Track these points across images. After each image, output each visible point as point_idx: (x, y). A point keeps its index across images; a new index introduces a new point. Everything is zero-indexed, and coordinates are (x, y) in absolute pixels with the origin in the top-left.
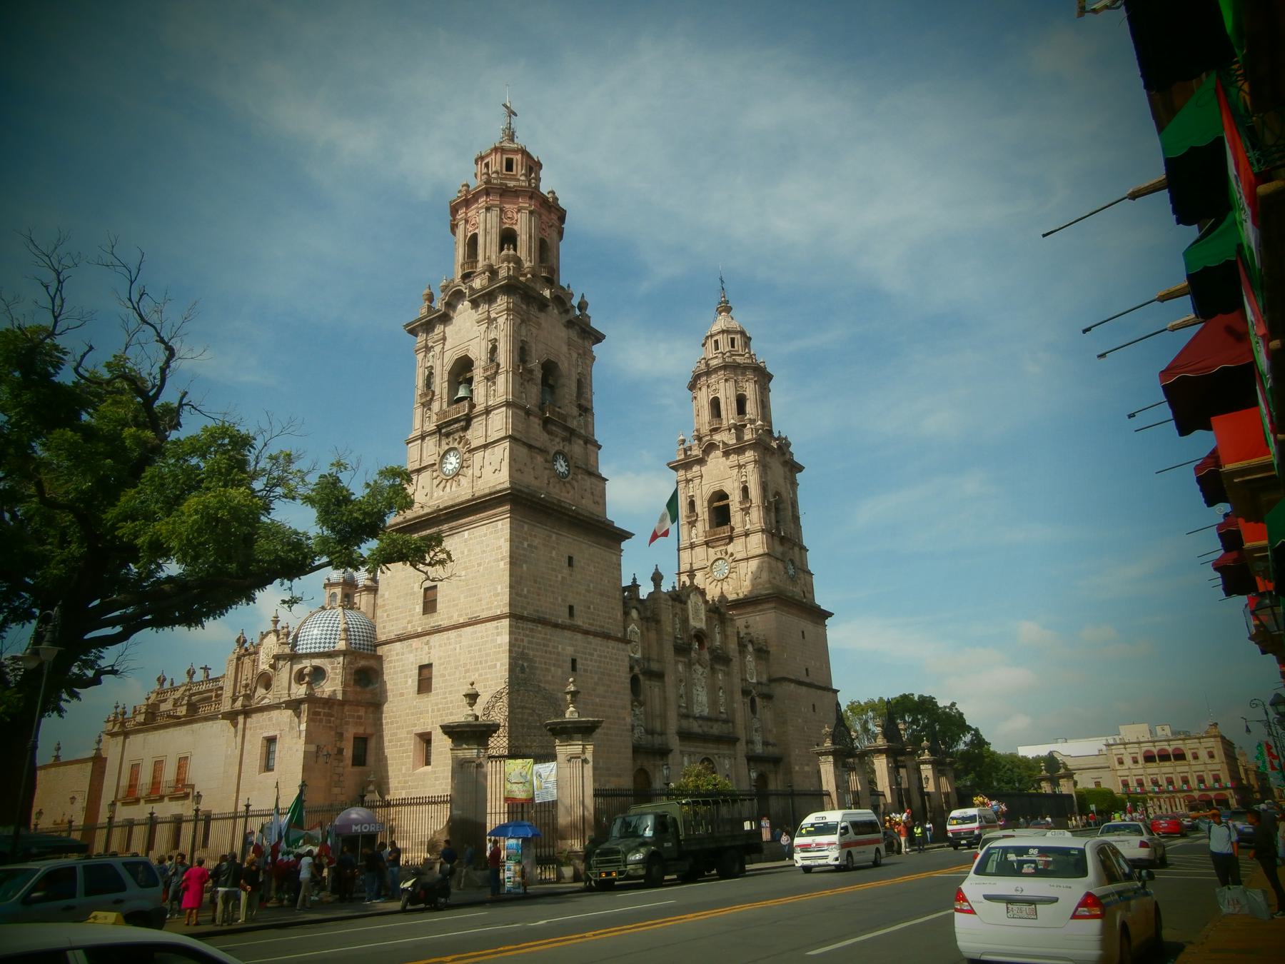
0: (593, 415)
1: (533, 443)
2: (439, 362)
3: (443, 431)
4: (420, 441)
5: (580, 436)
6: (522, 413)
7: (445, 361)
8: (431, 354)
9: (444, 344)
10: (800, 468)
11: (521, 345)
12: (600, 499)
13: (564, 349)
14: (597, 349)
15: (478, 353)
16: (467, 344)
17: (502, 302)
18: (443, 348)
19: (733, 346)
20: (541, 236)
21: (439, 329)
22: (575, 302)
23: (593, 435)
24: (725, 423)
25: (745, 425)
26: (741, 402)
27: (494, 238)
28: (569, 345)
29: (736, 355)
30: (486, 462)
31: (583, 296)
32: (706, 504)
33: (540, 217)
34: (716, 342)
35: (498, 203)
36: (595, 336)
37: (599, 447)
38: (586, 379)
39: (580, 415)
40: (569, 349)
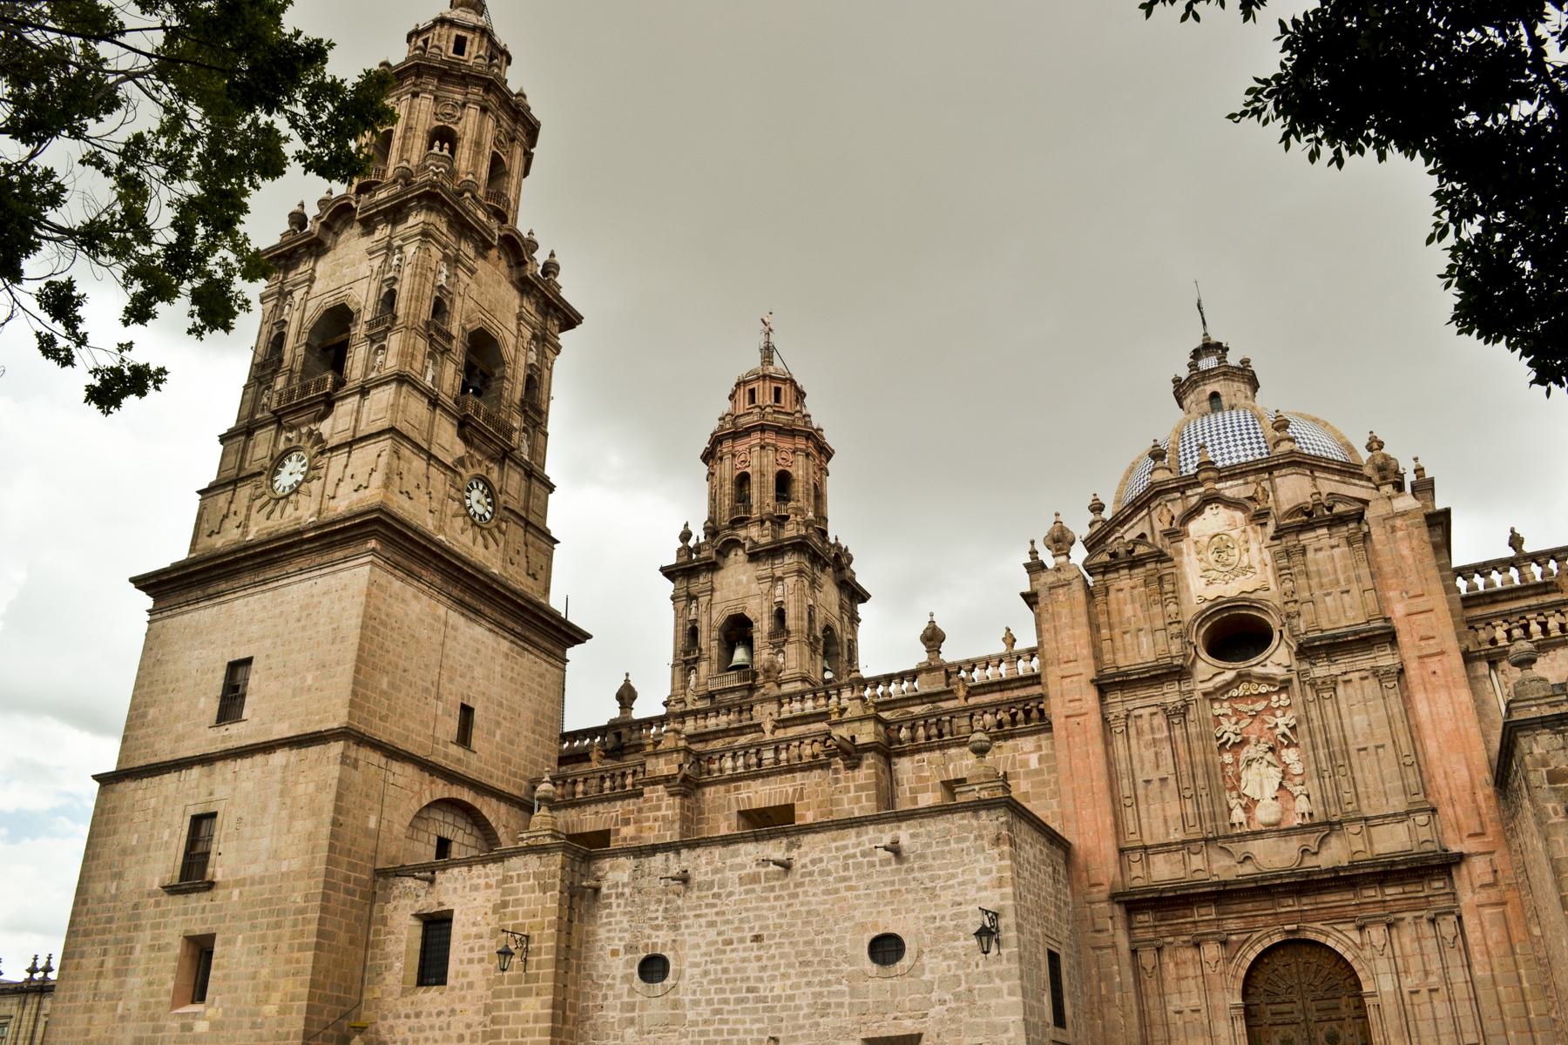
0: (546, 435)
1: (435, 451)
5: (519, 463)
7: (307, 315)
9: (310, 287)
10: (863, 597)
12: (542, 573)
15: (364, 298)
17: (416, 220)
18: (307, 293)
19: (777, 399)
20: (494, 149)
22: (541, 257)
24: (755, 513)
25: (787, 518)
26: (783, 482)
29: (779, 412)
32: (715, 634)
33: (498, 121)
34: (752, 392)
37: (551, 488)
39: (525, 430)
40: (519, 324)
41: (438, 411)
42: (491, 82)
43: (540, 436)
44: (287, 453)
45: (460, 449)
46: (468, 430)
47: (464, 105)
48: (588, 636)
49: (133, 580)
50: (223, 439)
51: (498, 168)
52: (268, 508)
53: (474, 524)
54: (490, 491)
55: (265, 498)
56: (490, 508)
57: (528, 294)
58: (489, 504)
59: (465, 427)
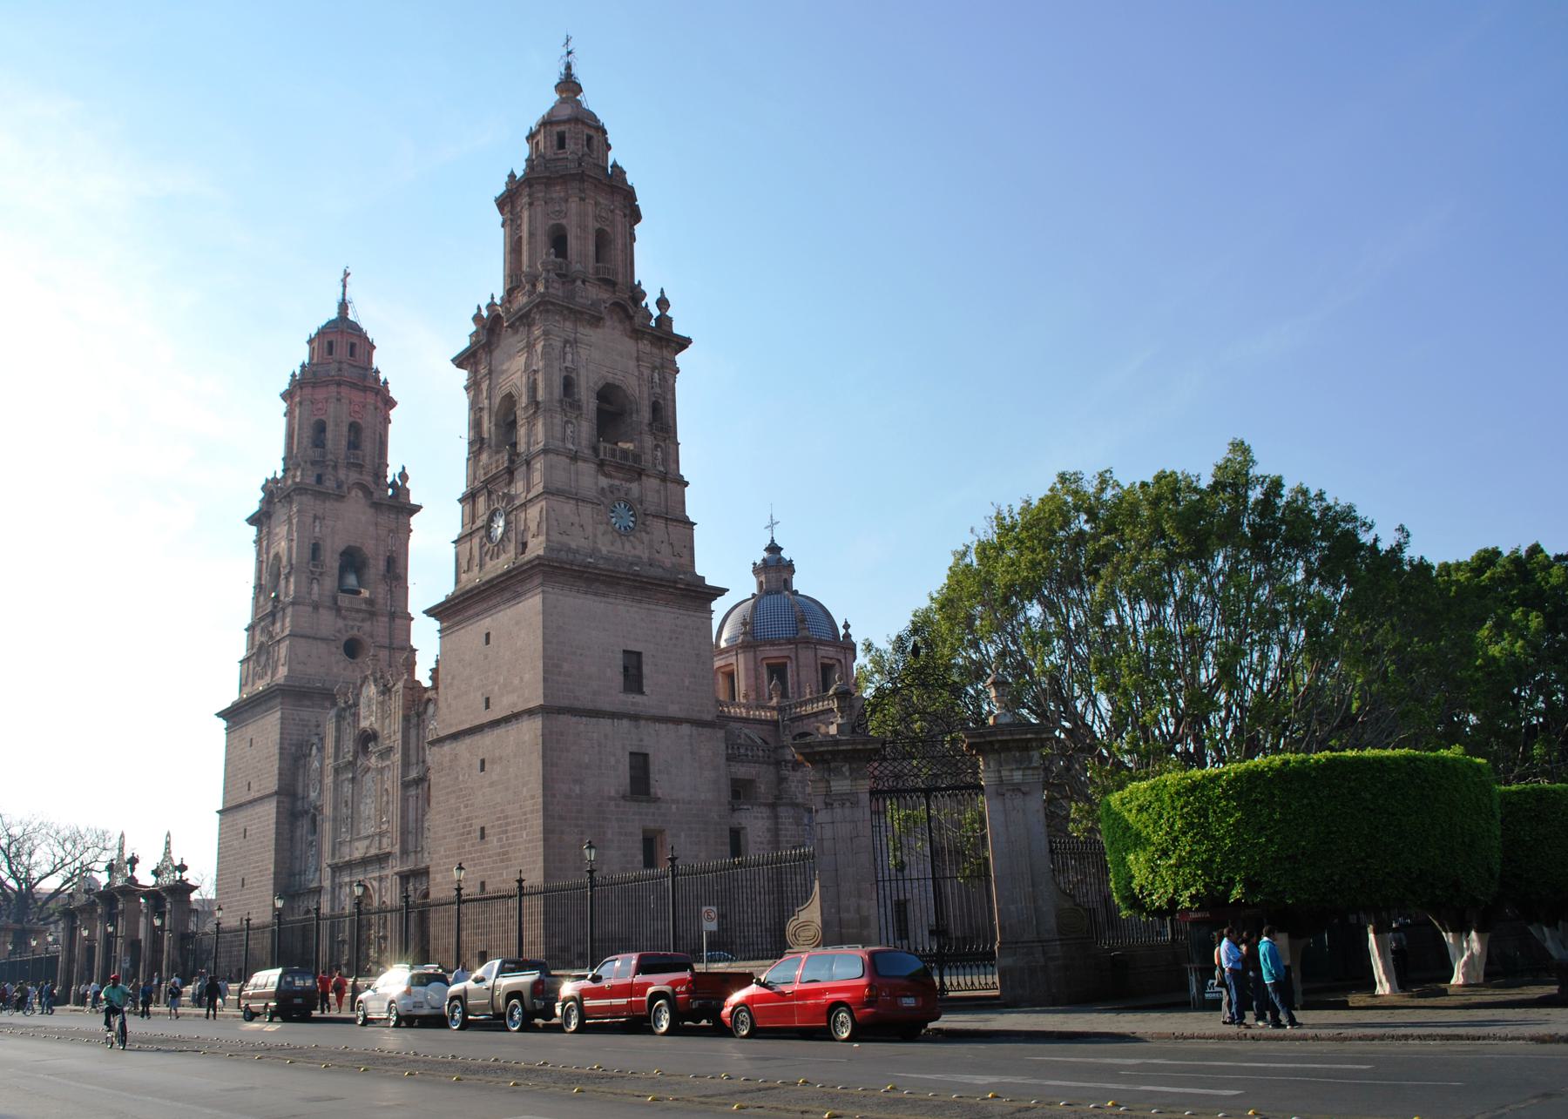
6: (564, 461)
11: (564, 373)
13: (632, 364)
14: (681, 359)
20: (599, 226)
22: (650, 302)
28: (638, 359)
37: (687, 484)
38: (664, 399)
39: (657, 446)
43: (672, 446)
45: (604, 482)
46: (606, 468)
47: (567, 201)
48: (728, 590)
49: (424, 612)
50: (461, 501)
51: (602, 241)
53: (620, 535)
56: (633, 519)
57: (641, 339)
58: (632, 516)
59: (601, 465)
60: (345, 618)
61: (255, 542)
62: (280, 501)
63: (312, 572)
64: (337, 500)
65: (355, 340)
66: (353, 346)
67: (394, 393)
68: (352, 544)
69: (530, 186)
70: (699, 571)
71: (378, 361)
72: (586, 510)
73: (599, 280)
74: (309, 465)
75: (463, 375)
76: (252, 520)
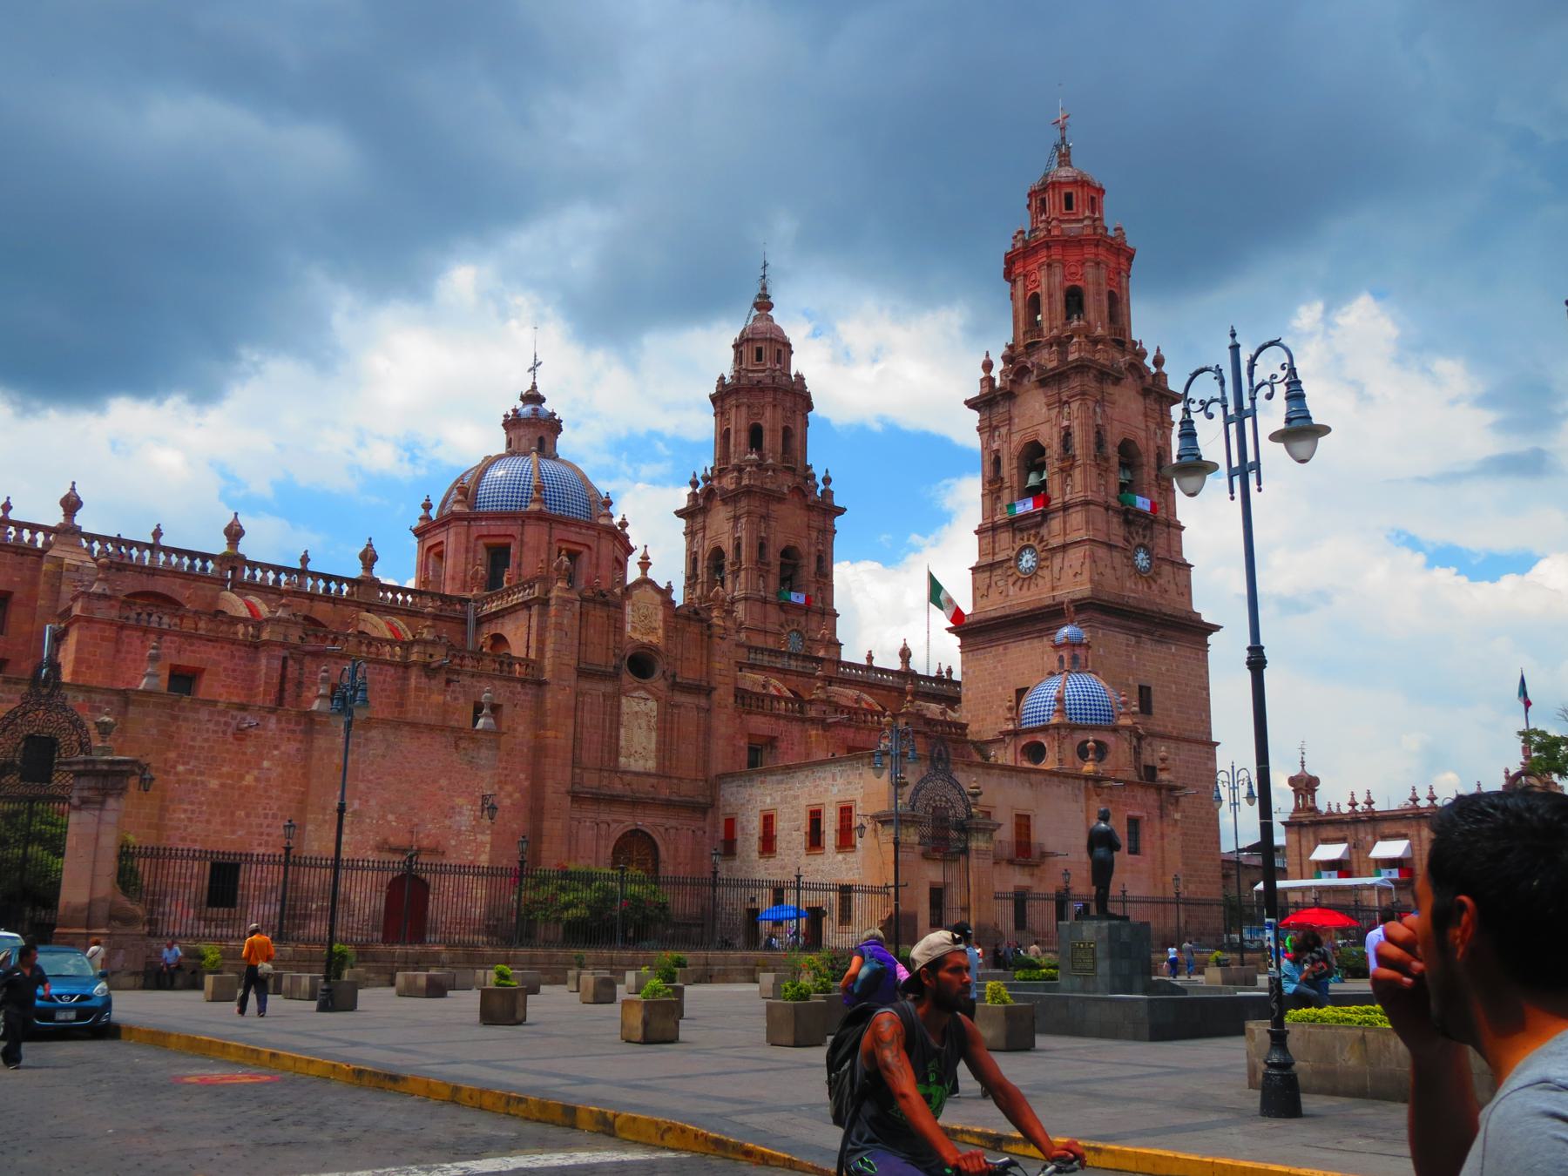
2: (1005, 446)
3: (1016, 525)
4: (990, 533)
8: (997, 433)
9: (1009, 424)
15: (1049, 438)
16: (1038, 427)
20: (1109, 288)
21: (1001, 409)
22: (1148, 362)
23: (1175, 516)
27: (1059, 297)
28: (1146, 415)
30: (1066, 564)
31: (1158, 350)
35: (1060, 257)
36: (1173, 399)
37: (1182, 528)
41: (1110, 512)
42: (1098, 241)
44: (1023, 548)
50: (977, 532)
52: (1019, 583)
54: (1149, 551)
55: (1014, 578)
60: (785, 612)
61: (685, 534)
62: (723, 500)
63: (760, 570)
64: (779, 503)
65: (782, 348)
66: (779, 351)
67: (814, 400)
68: (792, 544)
69: (1049, 248)
70: (1197, 607)
71: (797, 365)
72: (1117, 557)
73: (1114, 340)
74: (754, 469)
75: (974, 416)
76: (680, 513)
